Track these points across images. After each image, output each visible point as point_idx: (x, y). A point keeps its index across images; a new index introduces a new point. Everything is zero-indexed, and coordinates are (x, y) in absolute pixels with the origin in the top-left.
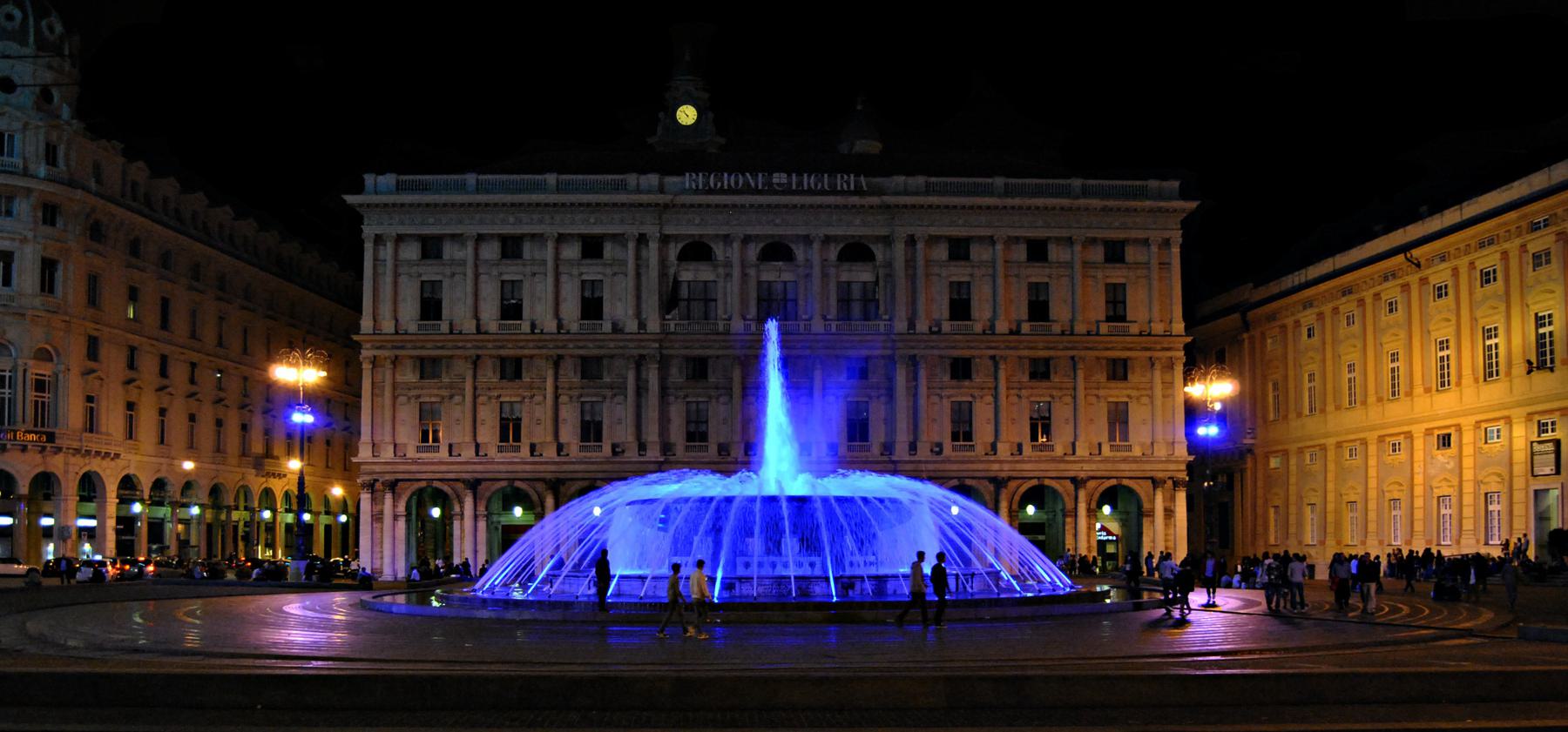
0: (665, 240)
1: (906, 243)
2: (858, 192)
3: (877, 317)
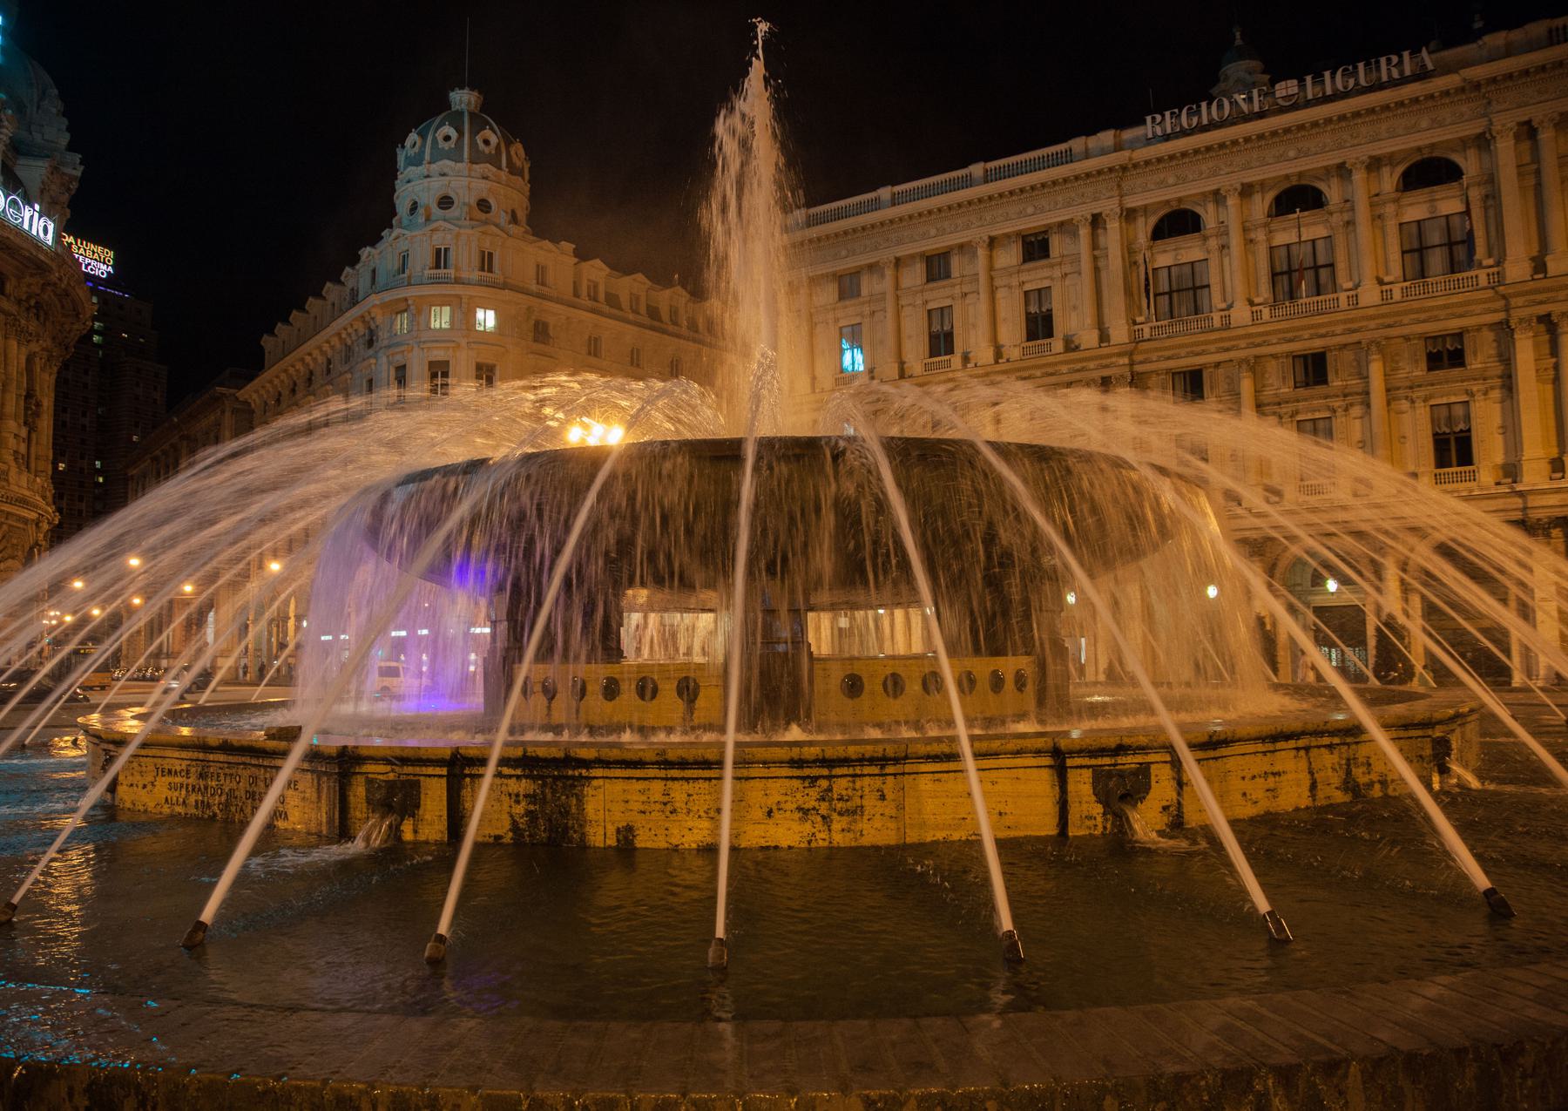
0: (1129, 215)
1: (1518, 138)
2: (1422, 75)
3: (1470, 263)
